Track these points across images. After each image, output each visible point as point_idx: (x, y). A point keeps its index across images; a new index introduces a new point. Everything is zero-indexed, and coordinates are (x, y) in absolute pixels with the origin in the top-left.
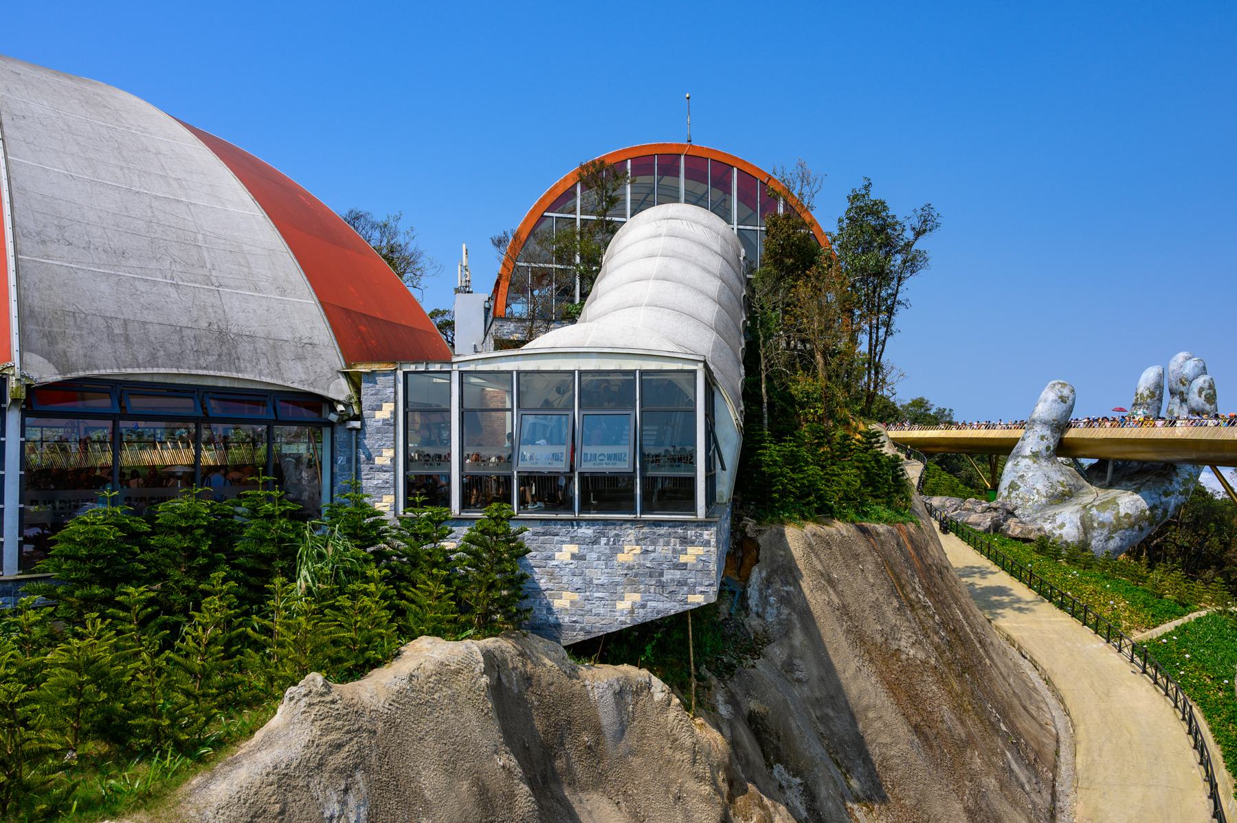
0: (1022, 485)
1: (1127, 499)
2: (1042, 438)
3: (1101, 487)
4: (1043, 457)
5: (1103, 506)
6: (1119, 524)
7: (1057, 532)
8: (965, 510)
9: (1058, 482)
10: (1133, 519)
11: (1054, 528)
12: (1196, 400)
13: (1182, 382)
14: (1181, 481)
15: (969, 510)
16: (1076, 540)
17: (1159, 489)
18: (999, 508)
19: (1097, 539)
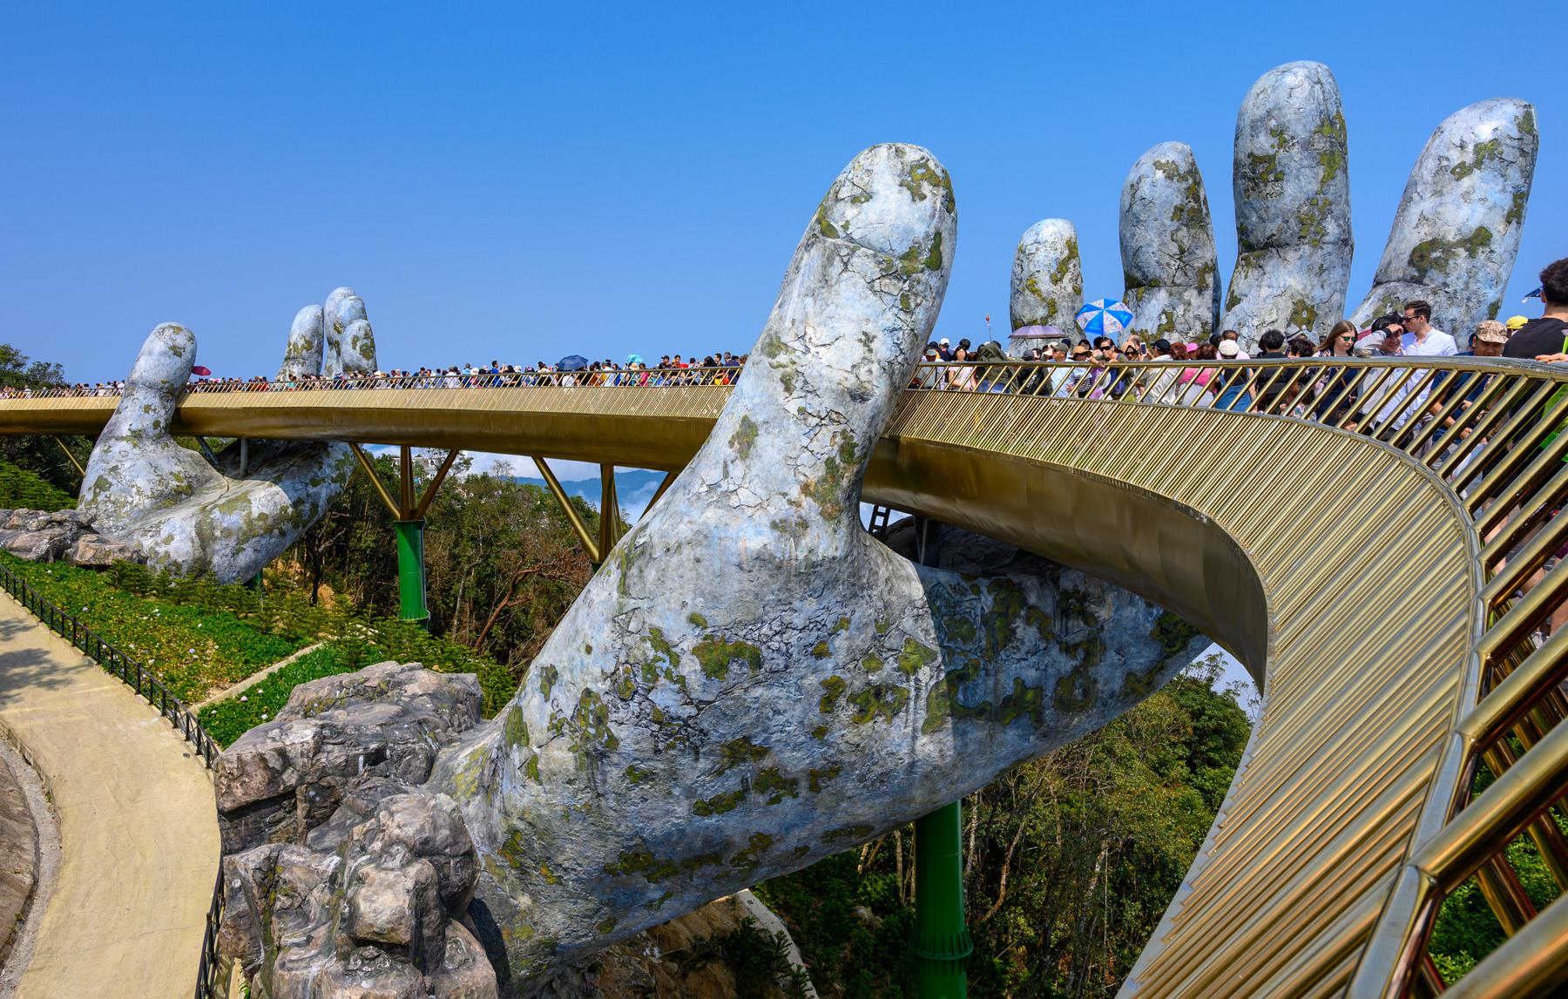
0: (115, 482)
1: (263, 493)
2: (147, 409)
3: (235, 478)
4: (148, 437)
5: (230, 505)
6: (251, 530)
7: (162, 550)
8: (12, 527)
9: (171, 473)
10: (270, 521)
11: (157, 544)
12: (351, 353)
13: (336, 329)
14: (333, 464)
15: (17, 527)
16: (189, 558)
17: (306, 476)
18: (65, 521)
19: (221, 553)
